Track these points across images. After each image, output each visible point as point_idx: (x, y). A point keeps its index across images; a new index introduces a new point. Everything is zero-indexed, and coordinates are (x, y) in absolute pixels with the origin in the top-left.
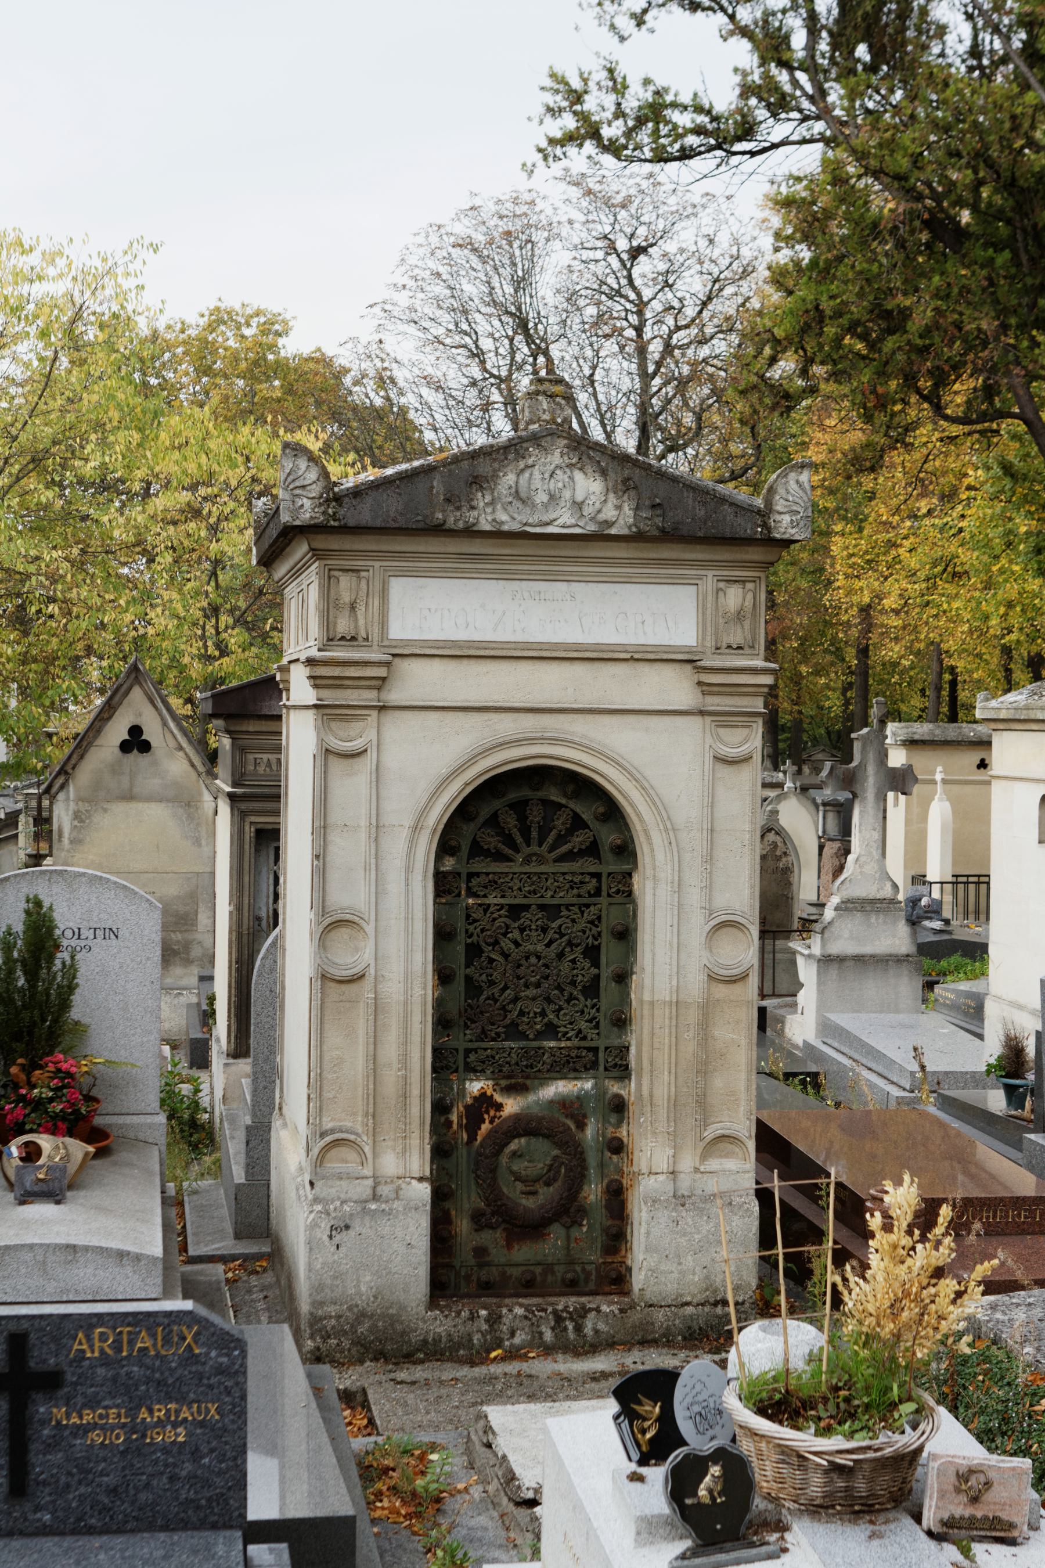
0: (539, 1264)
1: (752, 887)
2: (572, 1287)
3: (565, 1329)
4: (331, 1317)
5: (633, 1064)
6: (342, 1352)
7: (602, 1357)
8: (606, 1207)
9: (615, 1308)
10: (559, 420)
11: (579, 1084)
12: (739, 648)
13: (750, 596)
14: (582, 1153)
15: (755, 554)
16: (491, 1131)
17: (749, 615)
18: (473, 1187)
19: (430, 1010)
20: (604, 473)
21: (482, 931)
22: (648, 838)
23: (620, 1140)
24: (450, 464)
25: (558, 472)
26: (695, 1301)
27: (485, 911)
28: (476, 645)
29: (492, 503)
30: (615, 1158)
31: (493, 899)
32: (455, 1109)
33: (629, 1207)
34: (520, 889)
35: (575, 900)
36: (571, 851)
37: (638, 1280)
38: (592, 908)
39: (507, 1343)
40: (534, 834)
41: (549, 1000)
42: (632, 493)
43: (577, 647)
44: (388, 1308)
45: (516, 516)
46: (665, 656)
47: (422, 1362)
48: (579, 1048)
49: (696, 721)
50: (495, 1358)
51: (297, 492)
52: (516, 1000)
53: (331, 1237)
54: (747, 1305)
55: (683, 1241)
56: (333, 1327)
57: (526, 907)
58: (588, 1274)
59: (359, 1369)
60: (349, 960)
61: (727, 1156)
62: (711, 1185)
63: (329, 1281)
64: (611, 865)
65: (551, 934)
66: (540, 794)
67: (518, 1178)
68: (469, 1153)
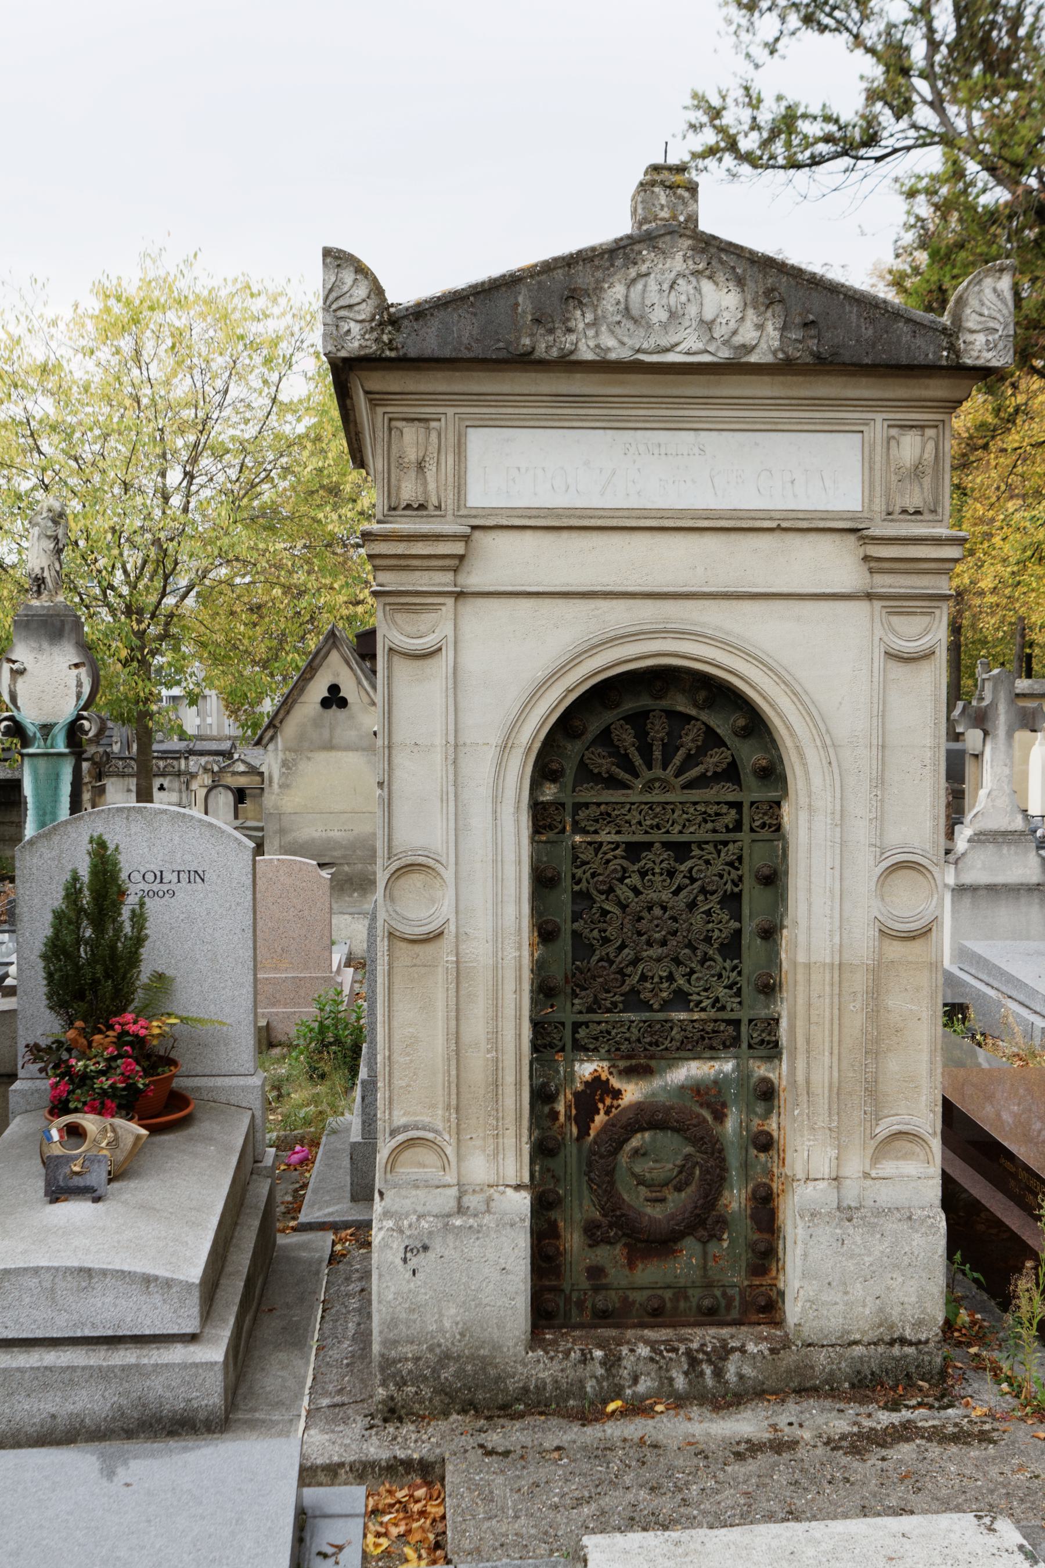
0: (669, 1287)
1: (936, 818)
2: (711, 1316)
3: (702, 1374)
4: (407, 1359)
5: (784, 1041)
7: (748, 1414)
8: (753, 1217)
9: (764, 1347)
10: (682, 218)
11: (717, 1065)
12: (918, 512)
13: (930, 446)
15: (938, 389)
16: (606, 1124)
17: (929, 471)
18: (586, 1192)
19: (527, 975)
20: (740, 282)
21: (593, 875)
22: (802, 756)
23: (769, 1135)
24: (539, 273)
25: (680, 281)
26: (866, 1339)
27: (597, 851)
28: (578, 513)
29: (595, 324)
30: (762, 1156)
32: (562, 1098)
33: (781, 1216)
34: (640, 823)
35: (709, 837)
37: (793, 1311)
38: (731, 846)
39: (628, 1392)
40: (657, 754)
41: (677, 961)
42: (778, 308)
43: (708, 514)
44: (478, 1348)
45: (626, 340)
46: (822, 524)
47: (521, 1416)
48: (716, 1021)
49: (862, 607)
50: (614, 1412)
51: (342, 313)
52: (635, 962)
53: (405, 1260)
54: (932, 1344)
55: (850, 1265)
56: (410, 1372)
57: (648, 846)
58: (730, 1300)
59: (443, 1425)
60: (423, 914)
61: (905, 1157)
62: (885, 1195)
63: (403, 1316)
64: (754, 792)
65: (679, 880)
66: (665, 703)
67: (641, 1182)
68: (579, 1151)
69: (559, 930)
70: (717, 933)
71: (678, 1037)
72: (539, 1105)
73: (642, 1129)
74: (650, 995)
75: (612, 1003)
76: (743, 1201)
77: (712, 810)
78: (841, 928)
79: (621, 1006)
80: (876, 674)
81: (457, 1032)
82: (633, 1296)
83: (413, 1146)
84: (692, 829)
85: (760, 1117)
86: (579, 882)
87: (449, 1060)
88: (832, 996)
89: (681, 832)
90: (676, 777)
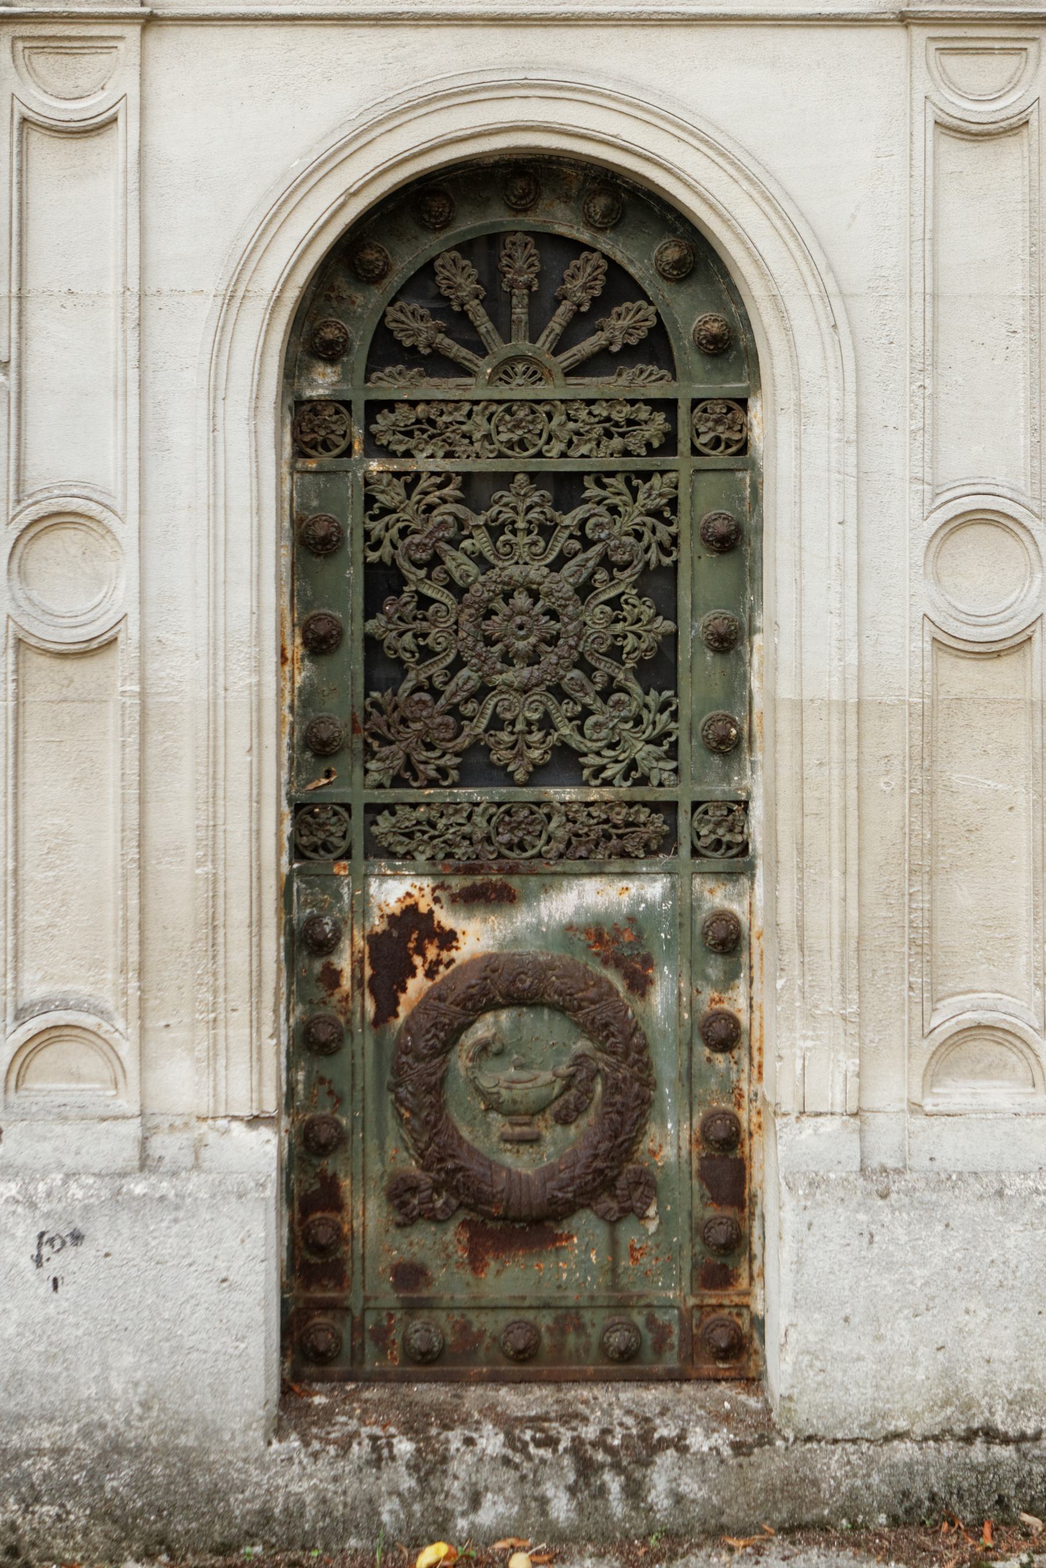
0: (546, 1306)
4: (41, 1453)
5: (758, 843)
6: (68, 1536)
11: (633, 886)
14: (642, 1049)
16: (428, 995)
18: (392, 1123)
21: (404, 533)
22: (782, 314)
23: (732, 1020)
27: (409, 488)
30: (720, 1060)
31: (426, 461)
32: (345, 944)
34: (487, 437)
35: (616, 463)
36: (604, 352)
37: (782, 1365)
38: (656, 480)
40: (520, 312)
41: (559, 693)
44: (176, 1433)
48: (631, 804)
52: (481, 693)
53: (38, 1261)
56: (47, 1476)
57: (506, 479)
58: (662, 1334)
63: (35, 1367)
64: (697, 382)
65: (561, 542)
66: (532, 220)
67: (493, 1105)
68: (379, 1045)
69: (341, 634)
70: (631, 640)
71: (560, 833)
72: (303, 960)
73: (494, 1006)
74: (508, 754)
75: (440, 770)
76: (685, 1145)
77: (620, 414)
78: (859, 634)
79: (454, 774)
80: (918, 162)
81: (141, 827)
82: (480, 1322)
83: (50, 1042)
84: (584, 450)
85: (715, 985)
86: (376, 546)
87: (125, 877)
88: (845, 762)
89: (563, 455)
90: (556, 352)
